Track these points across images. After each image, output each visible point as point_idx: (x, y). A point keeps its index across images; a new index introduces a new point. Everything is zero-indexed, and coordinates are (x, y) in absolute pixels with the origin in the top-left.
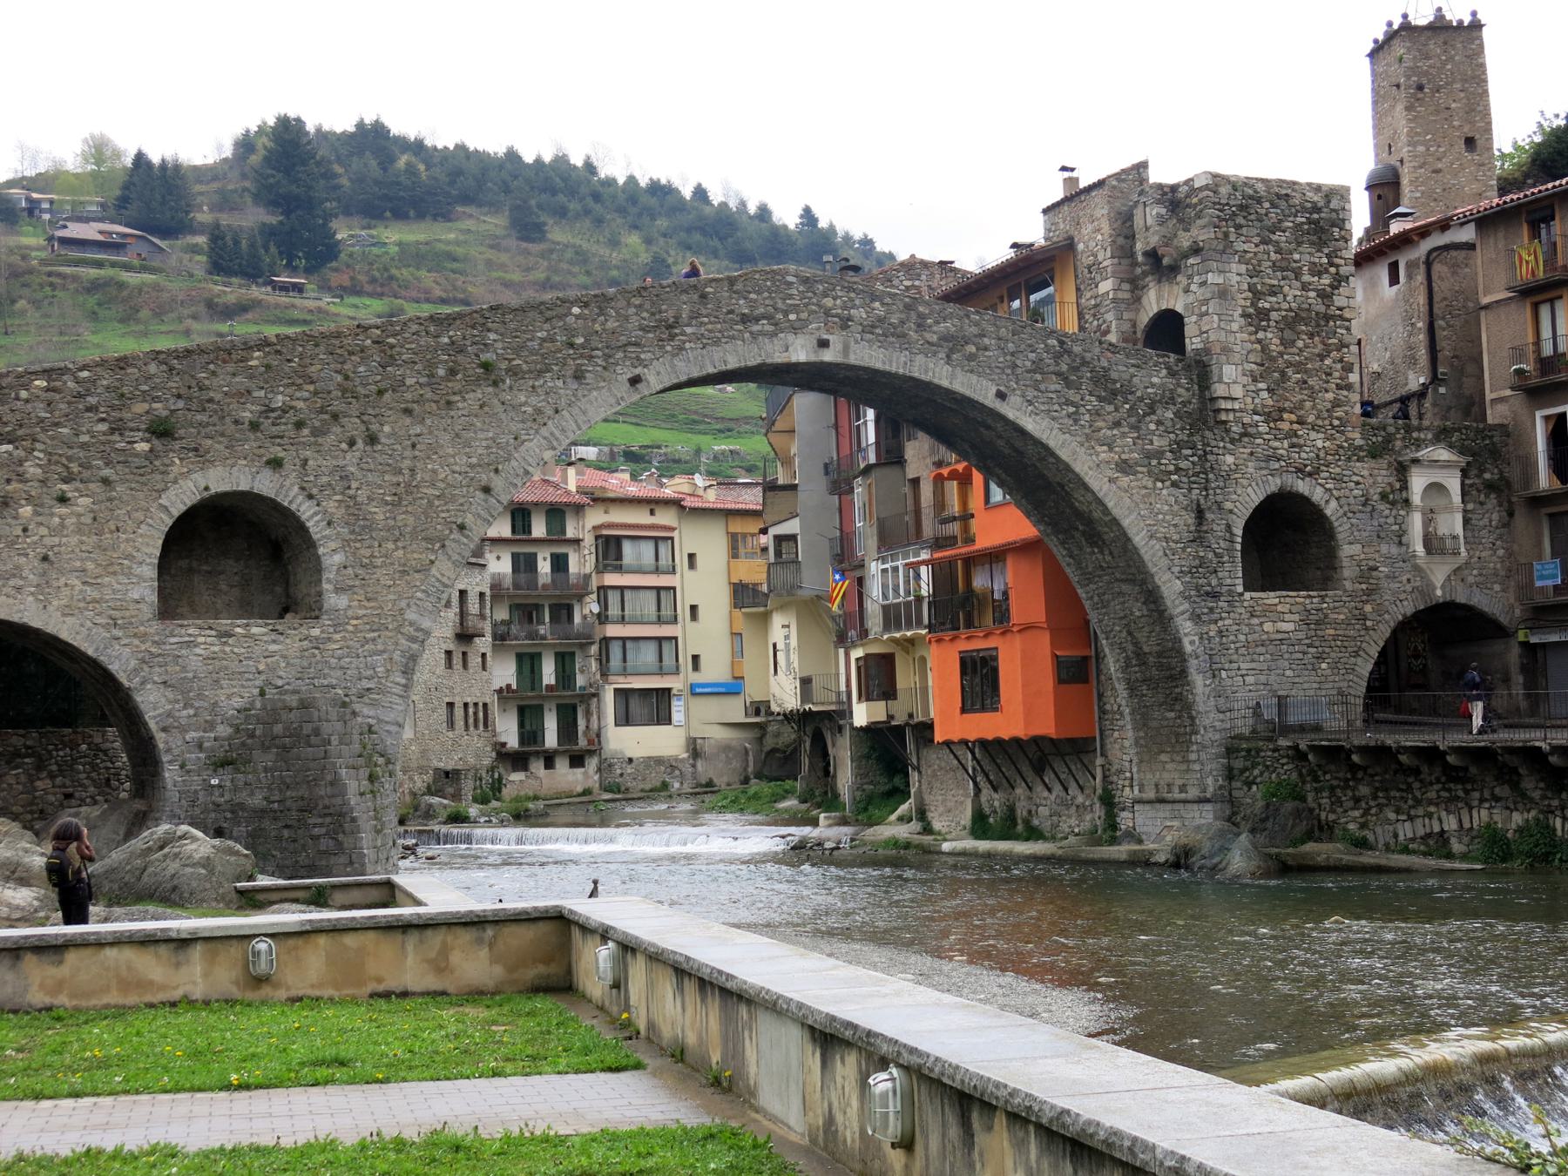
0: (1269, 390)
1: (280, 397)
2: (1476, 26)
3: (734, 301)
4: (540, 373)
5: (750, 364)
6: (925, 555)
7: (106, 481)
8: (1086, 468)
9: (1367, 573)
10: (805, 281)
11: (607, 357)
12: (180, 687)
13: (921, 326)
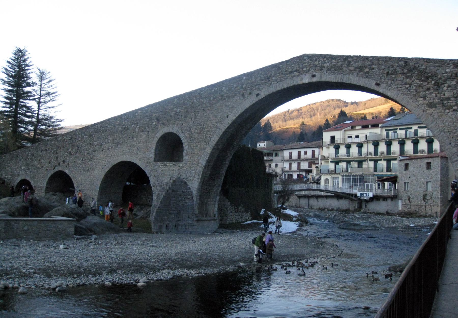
1: (179, 109)
3: (287, 68)
4: (234, 96)
5: (290, 86)
7: (148, 132)
8: (412, 107)
11: (251, 89)
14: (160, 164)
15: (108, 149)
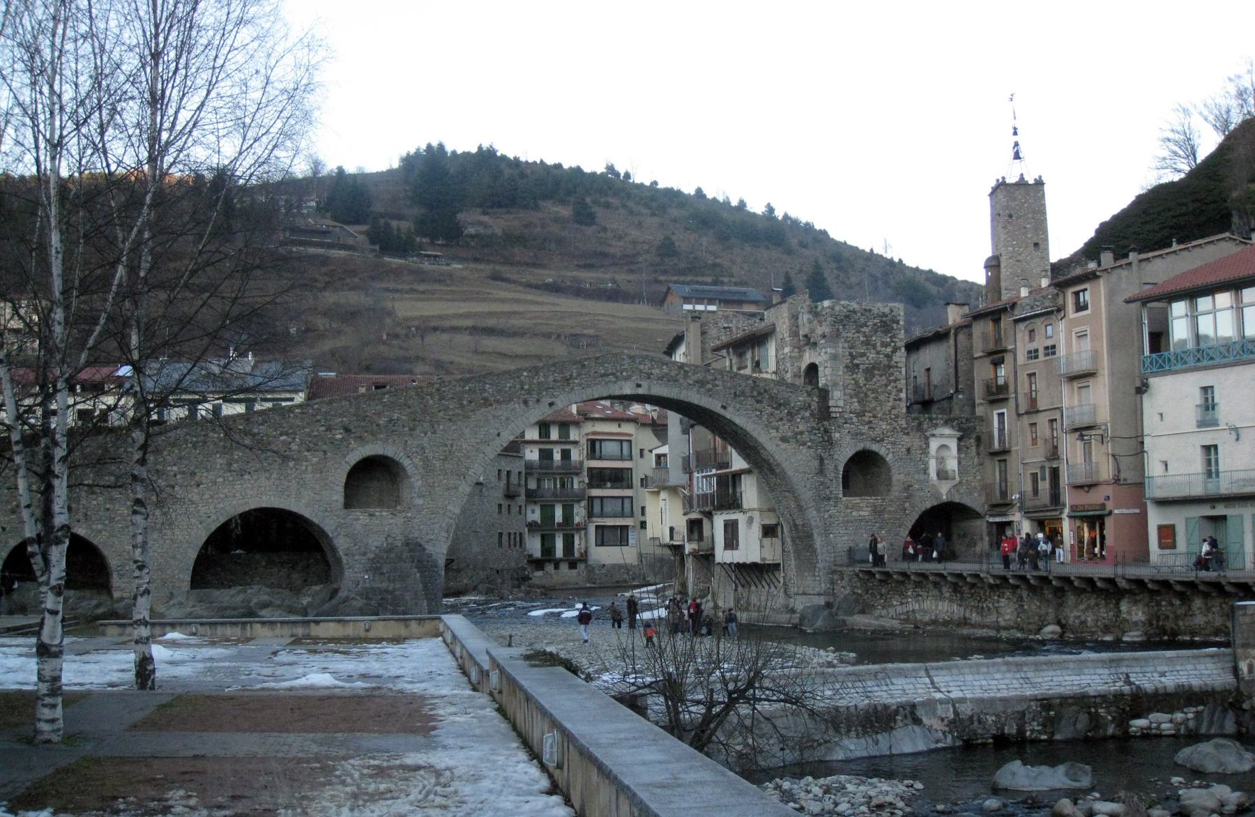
0: (859, 402)
2: (1039, 183)
6: (714, 471)
7: (325, 452)
9: (908, 487)
10: (631, 357)
11: (538, 394)
14: (358, 513)
15: (215, 483)
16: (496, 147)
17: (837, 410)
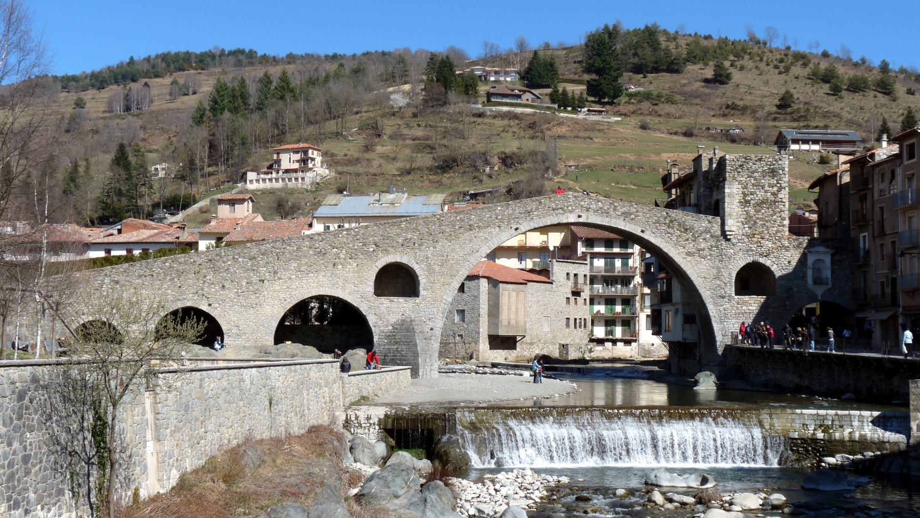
12: (379, 316)
13: (615, 210)
16: (658, 24)
17: (730, 233)
